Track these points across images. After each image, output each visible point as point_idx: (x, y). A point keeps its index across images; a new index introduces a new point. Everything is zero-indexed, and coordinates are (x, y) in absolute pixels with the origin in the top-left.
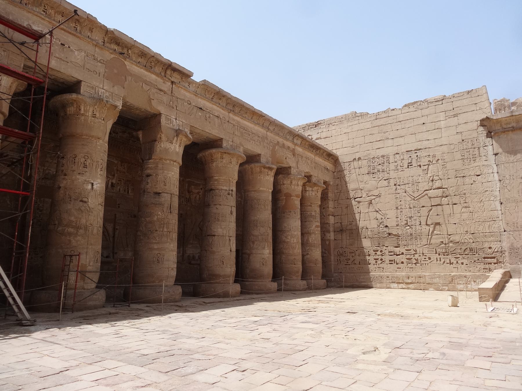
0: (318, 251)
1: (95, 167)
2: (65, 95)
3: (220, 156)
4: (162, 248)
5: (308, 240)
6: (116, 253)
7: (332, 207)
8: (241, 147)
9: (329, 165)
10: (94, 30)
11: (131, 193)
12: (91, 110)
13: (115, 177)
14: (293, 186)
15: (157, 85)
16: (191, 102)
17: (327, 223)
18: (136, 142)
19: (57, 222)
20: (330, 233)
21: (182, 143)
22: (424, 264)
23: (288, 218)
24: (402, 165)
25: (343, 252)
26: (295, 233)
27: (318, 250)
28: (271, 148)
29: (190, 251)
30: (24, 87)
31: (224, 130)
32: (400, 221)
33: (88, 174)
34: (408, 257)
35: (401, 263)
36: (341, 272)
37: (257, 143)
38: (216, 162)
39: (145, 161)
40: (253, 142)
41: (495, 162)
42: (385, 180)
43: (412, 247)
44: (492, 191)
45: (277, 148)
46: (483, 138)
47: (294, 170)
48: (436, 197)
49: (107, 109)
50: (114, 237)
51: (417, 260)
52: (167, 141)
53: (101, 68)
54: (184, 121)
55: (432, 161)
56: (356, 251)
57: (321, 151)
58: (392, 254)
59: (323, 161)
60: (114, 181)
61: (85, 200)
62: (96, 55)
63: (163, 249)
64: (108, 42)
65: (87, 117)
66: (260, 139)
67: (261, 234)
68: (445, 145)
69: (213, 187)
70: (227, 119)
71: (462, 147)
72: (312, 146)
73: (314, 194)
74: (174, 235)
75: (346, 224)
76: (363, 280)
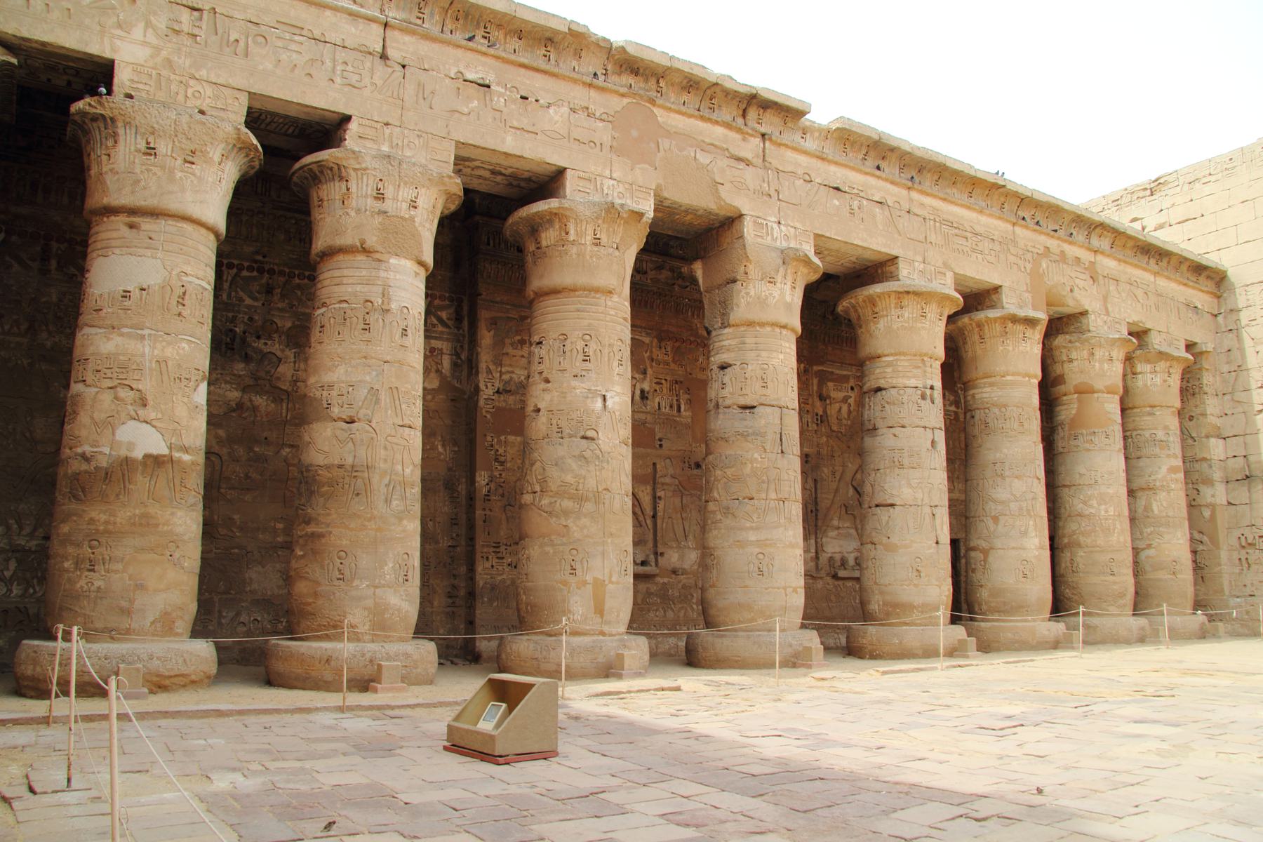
0: (1179, 536)
1: (606, 359)
2: (534, 204)
3: (894, 302)
4: (767, 540)
5: (1147, 508)
6: (662, 554)
8: (947, 274)
9: (1201, 299)
10: (583, 54)
11: (685, 411)
12: (590, 232)
13: (648, 376)
14: (1097, 364)
15: (727, 149)
16: (813, 175)
17: (1204, 459)
18: (688, 289)
19: (537, 488)
21: (798, 279)
23: (1088, 450)
25: (1257, 537)
26: (1110, 491)
27: (1179, 534)
28: (1029, 266)
29: (837, 545)
30: (457, 203)
31: (900, 235)
33: (593, 375)
37: (989, 258)
38: (886, 319)
39: (714, 333)
40: (979, 256)
45: (1044, 265)
47: (1098, 320)
49: (622, 222)
50: (654, 517)
52: (762, 280)
53: (604, 133)
54: (798, 225)
57: (1174, 260)
59: (1182, 288)
60: (646, 386)
61: (590, 434)
62: (591, 106)
63: (768, 542)
64: (613, 73)
65: (583, 247)
66: (997, 247)
67: (1015, 496)
69: (882, 383)
70: (906, 206)
72: (1143, 248)
73: (1158, 380)
74: (793, 507)
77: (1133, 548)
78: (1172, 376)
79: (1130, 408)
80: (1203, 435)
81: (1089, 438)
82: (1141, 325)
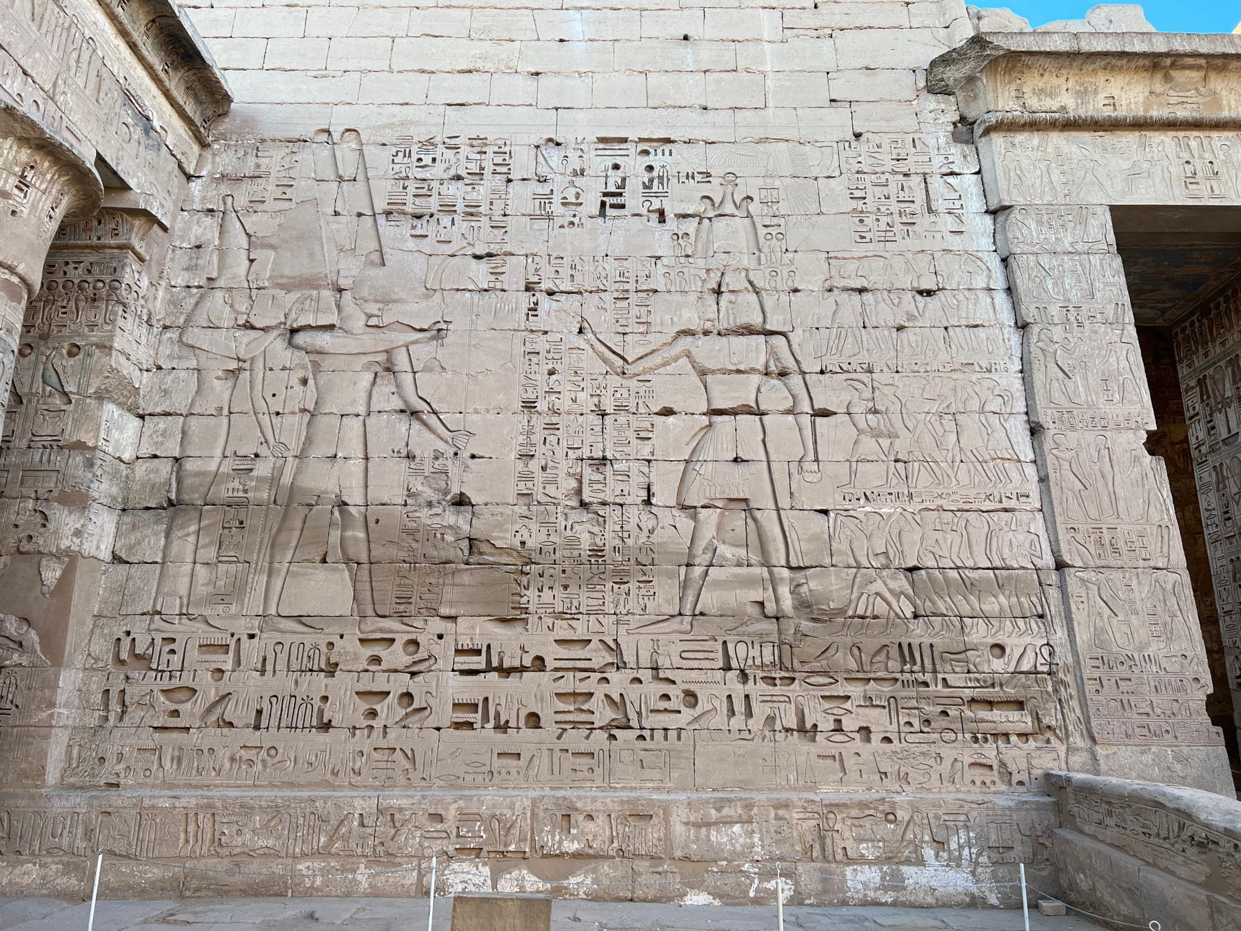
7: (143, 354)
17: (80, 446)
22: (659, 735)
25: (158, 642)
32: (539, 476)
34: (569, 683)
35: (522, 723)
41: (994, 243)
43: (594, 626)
46: (942, 140)
48: (730, 372)
51: (618, 704)
55: (717, 201)
58: (479, 662)
71: (854, 162)
76: (260, 843)
80: (91, 391)
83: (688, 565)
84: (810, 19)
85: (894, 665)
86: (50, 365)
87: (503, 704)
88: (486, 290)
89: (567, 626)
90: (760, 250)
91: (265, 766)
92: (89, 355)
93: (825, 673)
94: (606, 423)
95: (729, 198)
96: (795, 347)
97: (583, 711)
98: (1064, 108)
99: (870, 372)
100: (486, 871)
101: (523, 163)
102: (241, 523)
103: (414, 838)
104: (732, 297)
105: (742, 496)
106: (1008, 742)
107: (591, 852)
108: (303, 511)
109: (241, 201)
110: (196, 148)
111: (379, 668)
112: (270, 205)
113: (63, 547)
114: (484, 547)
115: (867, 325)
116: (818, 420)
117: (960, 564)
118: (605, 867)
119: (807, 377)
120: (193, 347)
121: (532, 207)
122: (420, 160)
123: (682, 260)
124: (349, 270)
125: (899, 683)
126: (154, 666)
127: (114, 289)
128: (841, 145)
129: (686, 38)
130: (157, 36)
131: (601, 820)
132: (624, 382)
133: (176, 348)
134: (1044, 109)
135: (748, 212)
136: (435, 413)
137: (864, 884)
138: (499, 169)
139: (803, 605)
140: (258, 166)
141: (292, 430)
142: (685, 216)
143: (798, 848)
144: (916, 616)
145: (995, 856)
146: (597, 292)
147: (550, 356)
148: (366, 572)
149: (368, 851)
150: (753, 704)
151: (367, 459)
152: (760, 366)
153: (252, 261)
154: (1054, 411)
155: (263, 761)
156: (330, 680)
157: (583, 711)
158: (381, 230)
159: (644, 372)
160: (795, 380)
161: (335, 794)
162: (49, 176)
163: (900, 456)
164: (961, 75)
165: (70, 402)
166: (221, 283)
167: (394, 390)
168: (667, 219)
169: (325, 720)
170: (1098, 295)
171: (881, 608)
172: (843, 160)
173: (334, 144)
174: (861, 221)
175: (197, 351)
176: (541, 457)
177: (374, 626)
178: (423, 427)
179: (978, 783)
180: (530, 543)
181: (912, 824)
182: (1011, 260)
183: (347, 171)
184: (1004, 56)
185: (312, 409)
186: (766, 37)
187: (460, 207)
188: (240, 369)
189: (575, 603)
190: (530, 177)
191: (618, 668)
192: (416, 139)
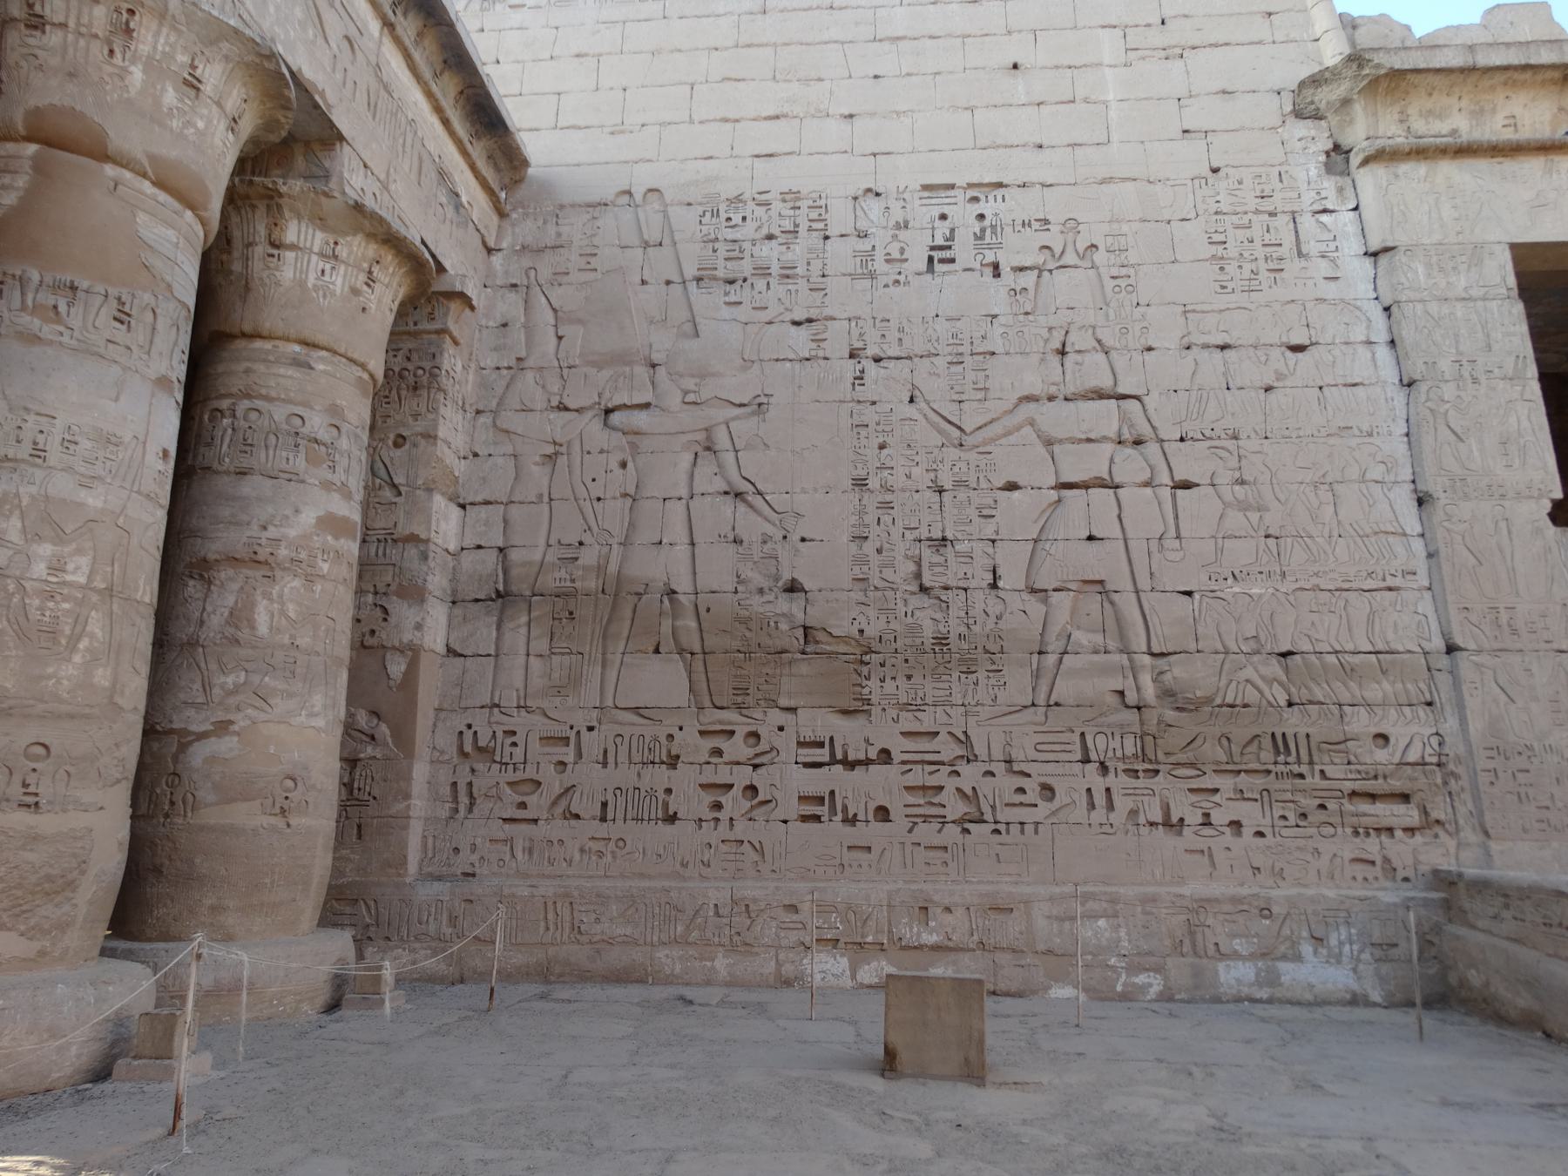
5: (240, 616)
7: (460, 441)
14: (137, 74)
17: (413, 539)
20: (423, 601)
22: (1015, 829)
23: (35, 339)
24: (896, 255)
25: (500, 735)
26: (93, 500)
27: (318, 700)
32: (875, 560)
34: (918, 776)
35: (871, 817)
36: (470, 871)
41: (1375, 289)
42: (797, 323)
43: (943, 719)
44: (1370, 435)
46: (1313, 172)
48: (1080, 441)
55: (1057, 251)
56: (584, 731)
58: (823, 755)
68: (1124, 179)
71: (1211, 201)
73: (339, 281)
75: (537, 556)
76: (619, 931)
77: (150, 732)
78: (377, 286)
79: (244, 335)
81: (47, 299)
82: (317, 98)
83: (1040, 653)
84: (1157, 38)
85: (1267, 755)
86: (378, 458)
87: (850, 797)
88: (808, 359)
89: (912, 718)
90: (1107, 305)
91: (614, 857)
92: (415, 445)
93: (1192, 765)
94: (944, 500)
95: (1070, 249)
96: (1151, 412)
97: (933, 804)
98: (1454, 132)
99: (1236, 438)
100: (844, 962)
101: (840, 218)
102: (571, 613)
103: (770, 928)
104: (1078, 357)
105: (1097, 578)
106: (1392, 836)
107: (951, 944)
108: (633, 599)
109: (545, 273)
110: (495, 218)
111: (720, 760)
112: (576, 277)
113: (405, 641)
114: (821, 636)
115: (1231, 386)
116: (1179, 492)
117: (1338, 648)
118: (966, 959)
119: (1166, 445)
120: (507, 432)
121: (852, 265)
122: (729, 219)
123: (1021, 318)
124: (661, 343)
125: (1273, 775)
126: (498, 758)
127: (433, 376)
128: (1196, 182)
129: (1015, 66)
130: (464, 107)
131: (959, 913)
132: (962, 455)
133: (491, 434)
134: (1432, 133)
135: (1093, 261)
136: (760, 493)
137: (1238, 981)
138: (815, 225)
139: (1167, 694)
140: (559, 235)
141: (614, 515)
142: (1021, 269)
143: (1167, 942)
144: (1290, 704)
145: (1378, 953)
146: (928, 356)
147: (880, 428)
148: (701, 663)
149: (726, 941)
150: (1115, 797)
151: (693, 544)
152: (1112, 433)
153: (560, 338)
154: (1445, 479)
155: (613, 852)
156: (672, 772)
157: (933, 804)
158: (692, 298)
159: (985, 444)
160: (1152, 449)
161: (685, 885)
162: (391, 270)
163: (1271, 531)
164: (1334, 97)
165: (400, 494)
166: (530, 363)
167: (716, 470)
168: (1002, 273)
169: (671, 813)
170: (1495, 347)
171: (1252, 696)
172: (1199, 199)
173: (637, 206)
174: (1222, 269)
175: (512, 436)
176: (876, 538)
177: (713, 718)
178: (748, 510)
179: (1360, 878)
180: (871, 631)
181: (1288, 921)
182: (1394, 309)
183: (653, 235)
184: (1386, 75)
185: (632, 493)
186: (1107, 61)
187: (775, 269)
188: (556, 454)
189: (920, 694)
190: (848, 232)
191: (968, 761)
192: (723, 197)
